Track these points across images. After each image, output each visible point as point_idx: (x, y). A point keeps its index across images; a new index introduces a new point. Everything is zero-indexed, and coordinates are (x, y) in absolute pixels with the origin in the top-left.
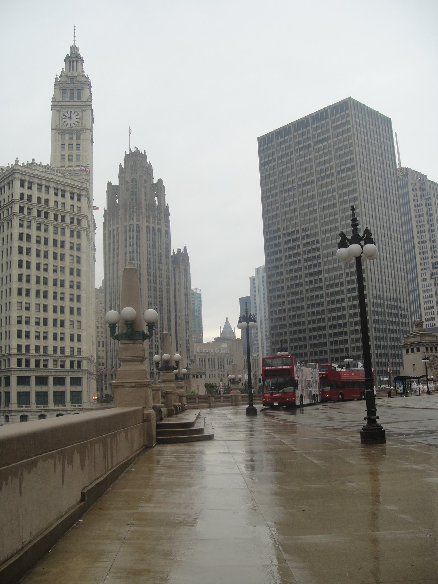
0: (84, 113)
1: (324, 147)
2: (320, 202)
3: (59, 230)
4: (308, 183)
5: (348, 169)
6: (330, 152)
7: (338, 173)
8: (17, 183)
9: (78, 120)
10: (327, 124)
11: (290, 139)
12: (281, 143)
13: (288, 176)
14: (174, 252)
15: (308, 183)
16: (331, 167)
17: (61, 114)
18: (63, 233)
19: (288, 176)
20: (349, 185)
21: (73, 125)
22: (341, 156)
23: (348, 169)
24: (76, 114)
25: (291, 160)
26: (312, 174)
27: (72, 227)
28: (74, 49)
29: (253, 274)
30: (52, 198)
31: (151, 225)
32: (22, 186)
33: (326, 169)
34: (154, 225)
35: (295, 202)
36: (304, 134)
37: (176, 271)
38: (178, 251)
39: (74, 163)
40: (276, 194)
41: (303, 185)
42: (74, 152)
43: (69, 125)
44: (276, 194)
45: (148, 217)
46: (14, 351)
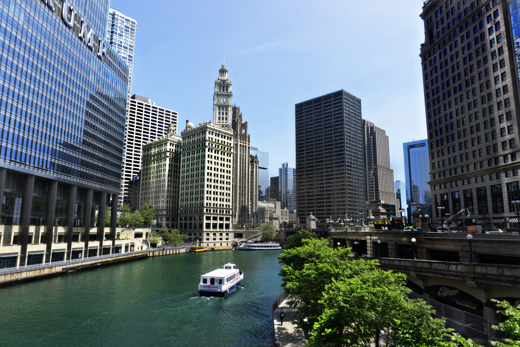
1: (329, 113)
2: (325, 139)
5: (340, 125)
6: (331, 115)
7: (335, 126)
11: (312, 107)
12: (307, 108)
13: (310, 125)
15: (320, 129)
16: (331, 123)
20: (340, 132)
23: (340, 125)
26: (322, 125)
28: (223, 66)
29: (281, 167)
31: (242, 144)
32: (209, 134)
35: (312, 138)
36: (319, 105)
41: (317, 130)
42: (225, 116)
46: (205, 205)
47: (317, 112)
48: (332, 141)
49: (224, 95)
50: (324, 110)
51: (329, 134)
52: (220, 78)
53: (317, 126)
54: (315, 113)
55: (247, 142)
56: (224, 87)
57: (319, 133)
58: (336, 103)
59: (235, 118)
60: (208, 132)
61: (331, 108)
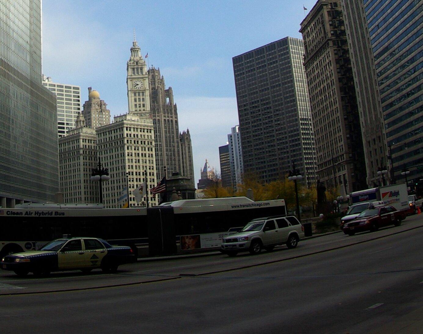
0: (145, 81)
3: (143, 149)
4: (266, 89)
8: (125, 129)
9: (142, 85)
10: (275, 52)
14: (180, 134)
15: (266, 89)
16: (279, 80)
17: (133, 82)
18: (145, 150)
21: (139, 88)
24: (141, 82)
25: (255, 74)
27: (148, 146)
29: (230, 132)
30: (139, 133)
31: (167, 119)
33: (276, 81)
34: (168, 118)
36: (261, 58)
37: (183, 146)
38: (183, 133)
40: (246, 96)
43: (138, 88)
44: (246, 96)
45: (164, 113)
49: (138, 78)
51: (278, 96)
53: (262, 86)
55: (173, 115)
59: (155, 84)
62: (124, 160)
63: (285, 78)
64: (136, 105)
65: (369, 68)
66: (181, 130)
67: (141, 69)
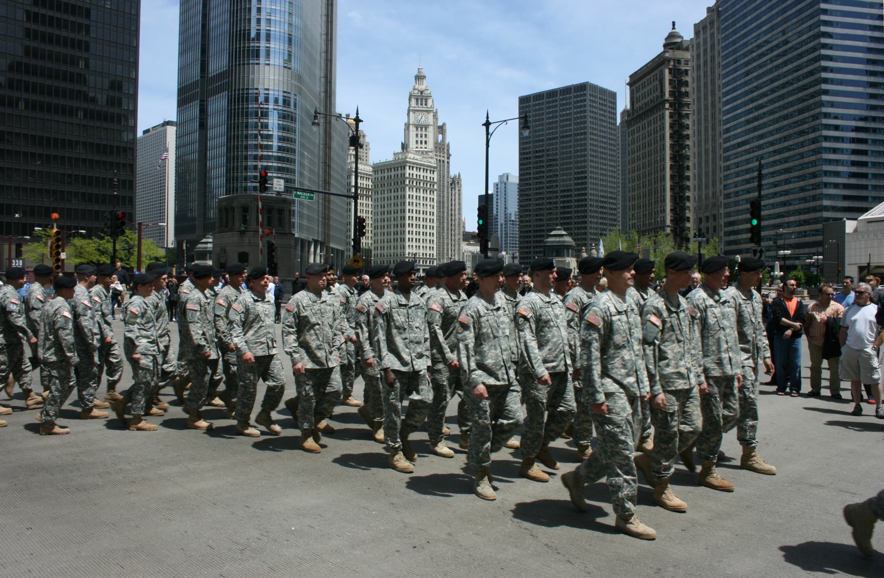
1: (567, 114)
4: (554, 138)
5: (582, 134)
6: (570, 119)
7: (575, 135)
8: (407, 168)
11: (543, 103)
13: (540, 130)
15: (554, 138)
16: (570, 130)
19: (540, 130)
22: (578, 124)
23: (582, 134)
26: (556, 133)
33: (567, 131)
36: (553, 101)
39: (424, 145)
41: (550, 139)
47: (550, 113)
48: (570, 158)
50: (561, 110)
52: (417, 87)
53: (550, 134)
54: (547, 113)
56: (422, 100)
57: (553, 144)
58: (578, 102)
60: (407, 168)
61: (570, 108)
62: (404, 203)
63: (578, 129)
64: (417, 142)
65: (714, 140)
66: (452, 174)
67: (426, 101)
